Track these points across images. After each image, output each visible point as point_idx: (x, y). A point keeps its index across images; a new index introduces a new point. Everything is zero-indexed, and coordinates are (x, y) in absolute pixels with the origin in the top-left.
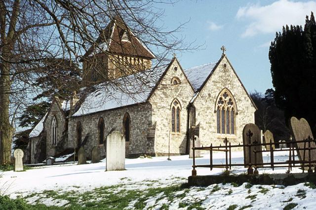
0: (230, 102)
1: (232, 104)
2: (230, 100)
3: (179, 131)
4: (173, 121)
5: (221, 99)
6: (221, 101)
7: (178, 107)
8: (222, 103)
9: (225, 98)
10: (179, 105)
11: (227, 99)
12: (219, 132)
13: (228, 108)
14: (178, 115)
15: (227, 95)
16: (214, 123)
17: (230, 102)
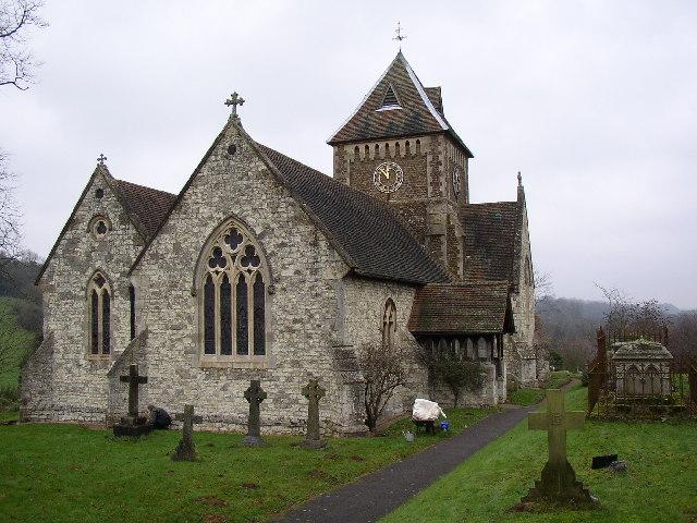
0: (250, 257)
1: (256, 261)
2: (250, 249)
3: (106, 350)
4: (95, 325)
5: (218, 251)
6: (218, 258)
7: (105, 291)
8: (223, 263)
9: (233, 247)
10: (106, 286)
11: (241, 247)
12: (210, 349)
13: (242, 277)
14: (107, 311)
15: (240, 239)
16: (190, 327)
17: (250, 257)
